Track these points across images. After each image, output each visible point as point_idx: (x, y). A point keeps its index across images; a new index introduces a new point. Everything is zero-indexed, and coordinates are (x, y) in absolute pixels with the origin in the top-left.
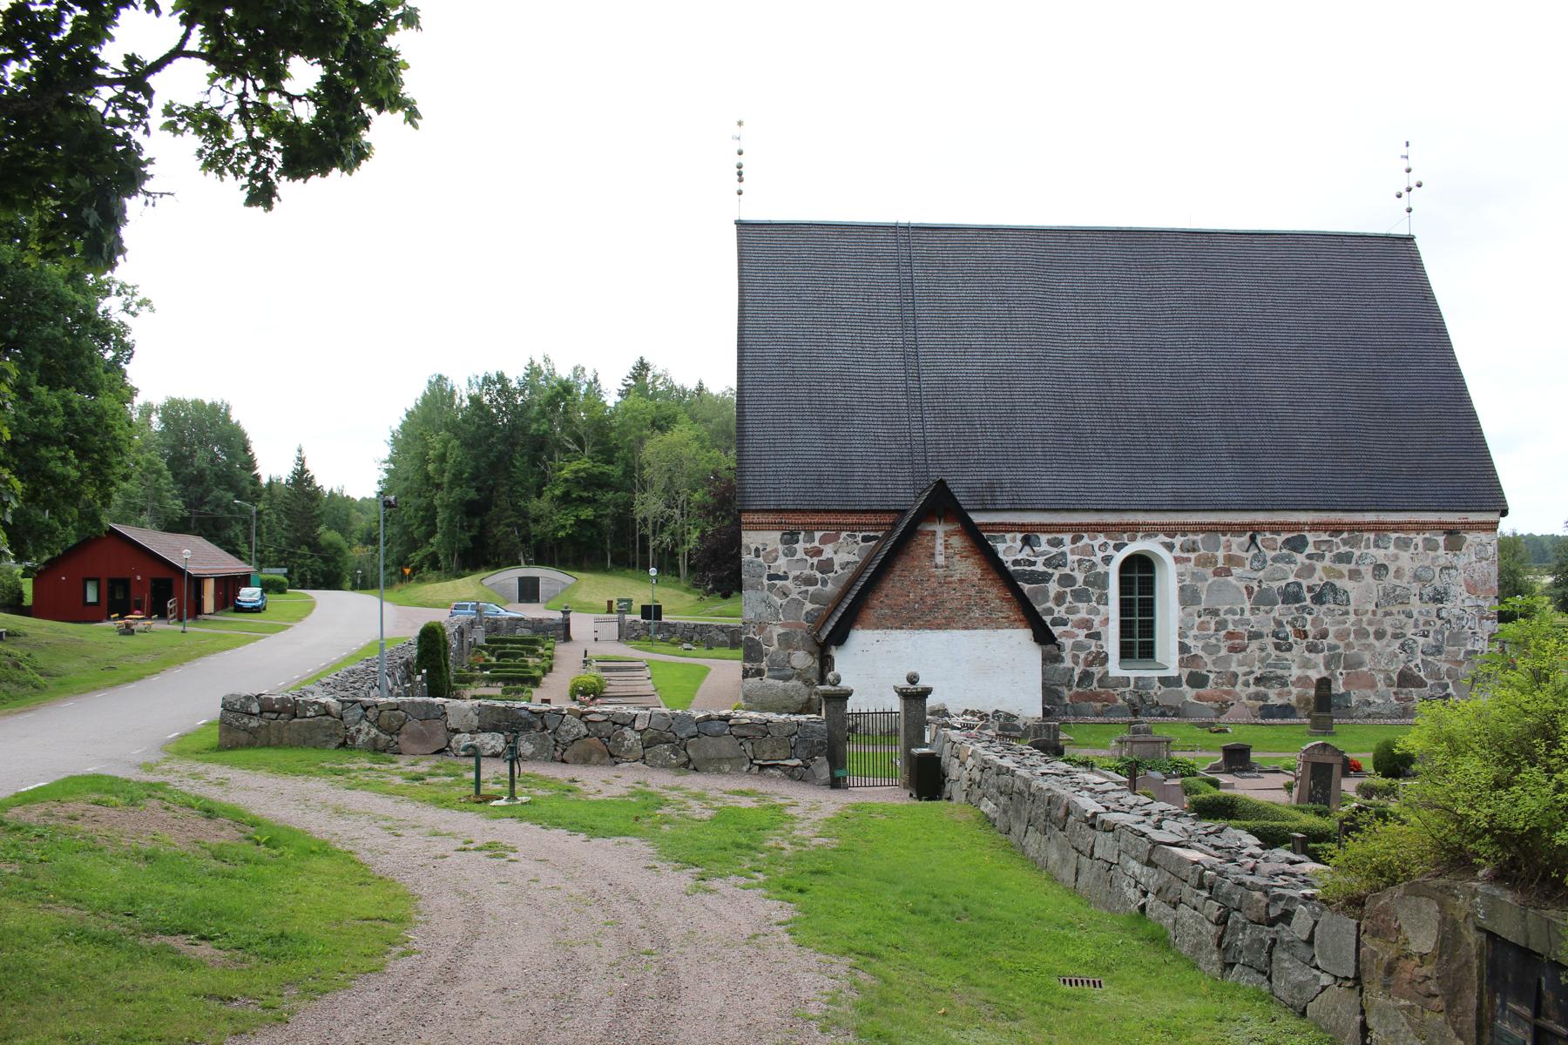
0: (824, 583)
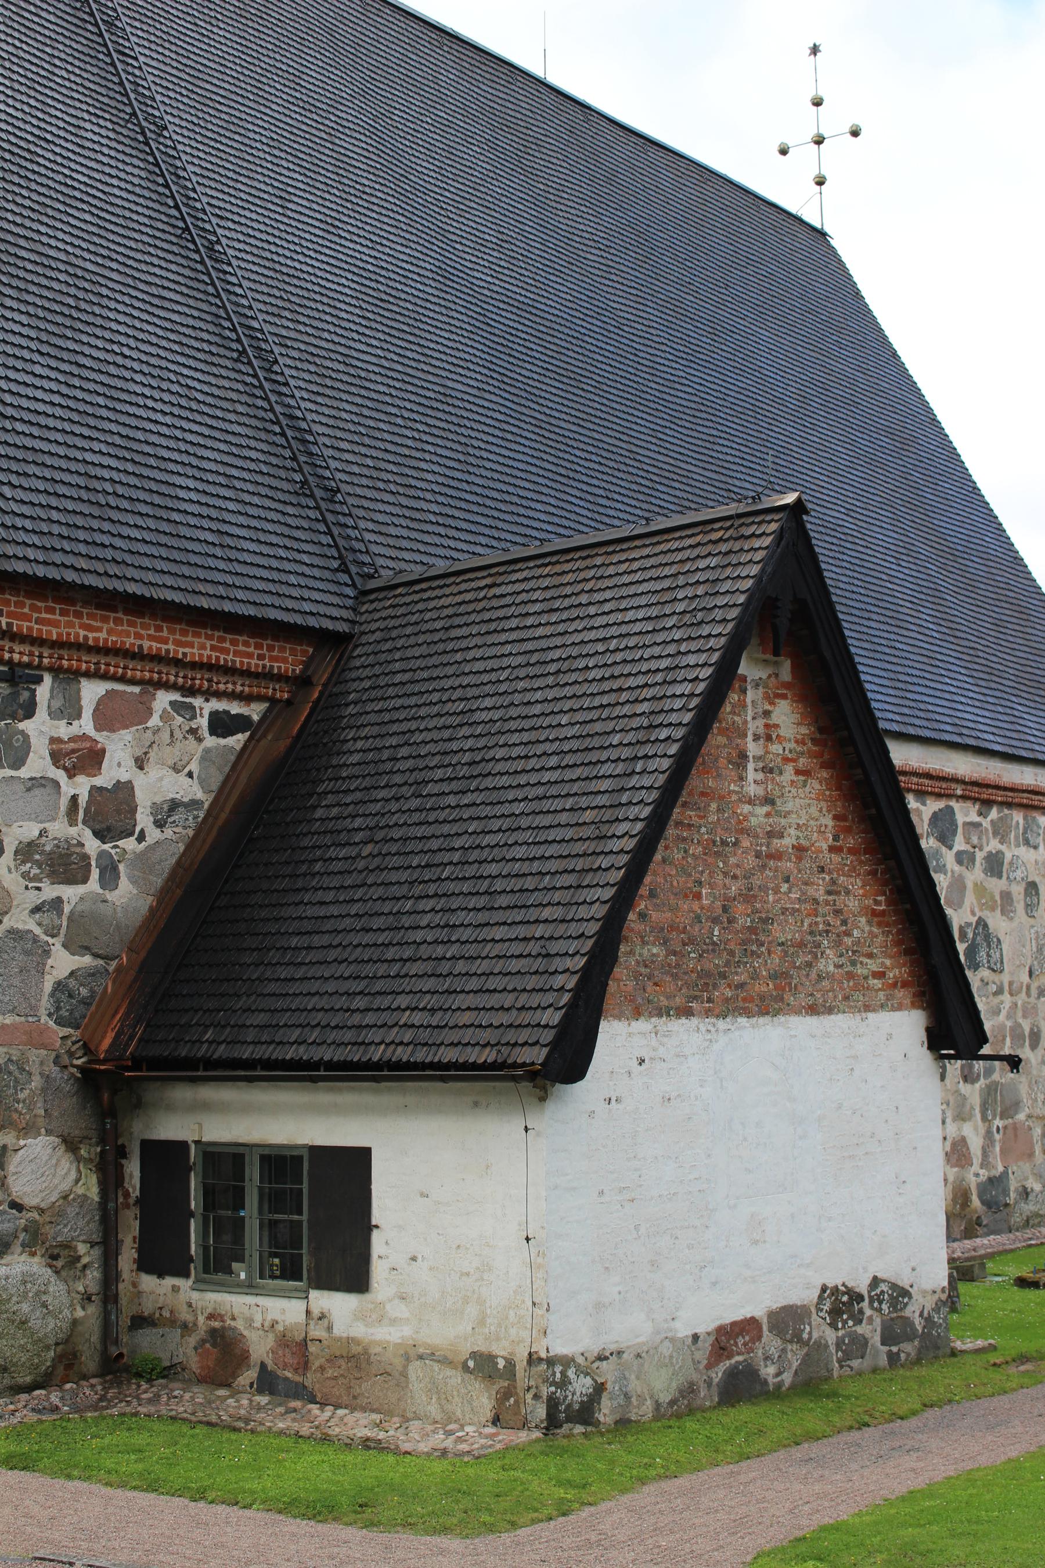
0: (110, 874)
